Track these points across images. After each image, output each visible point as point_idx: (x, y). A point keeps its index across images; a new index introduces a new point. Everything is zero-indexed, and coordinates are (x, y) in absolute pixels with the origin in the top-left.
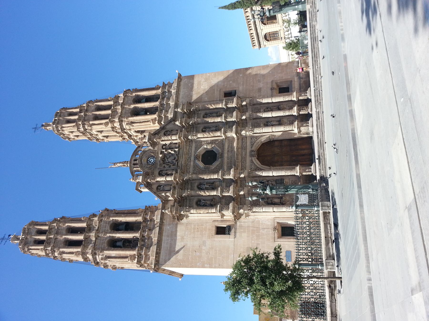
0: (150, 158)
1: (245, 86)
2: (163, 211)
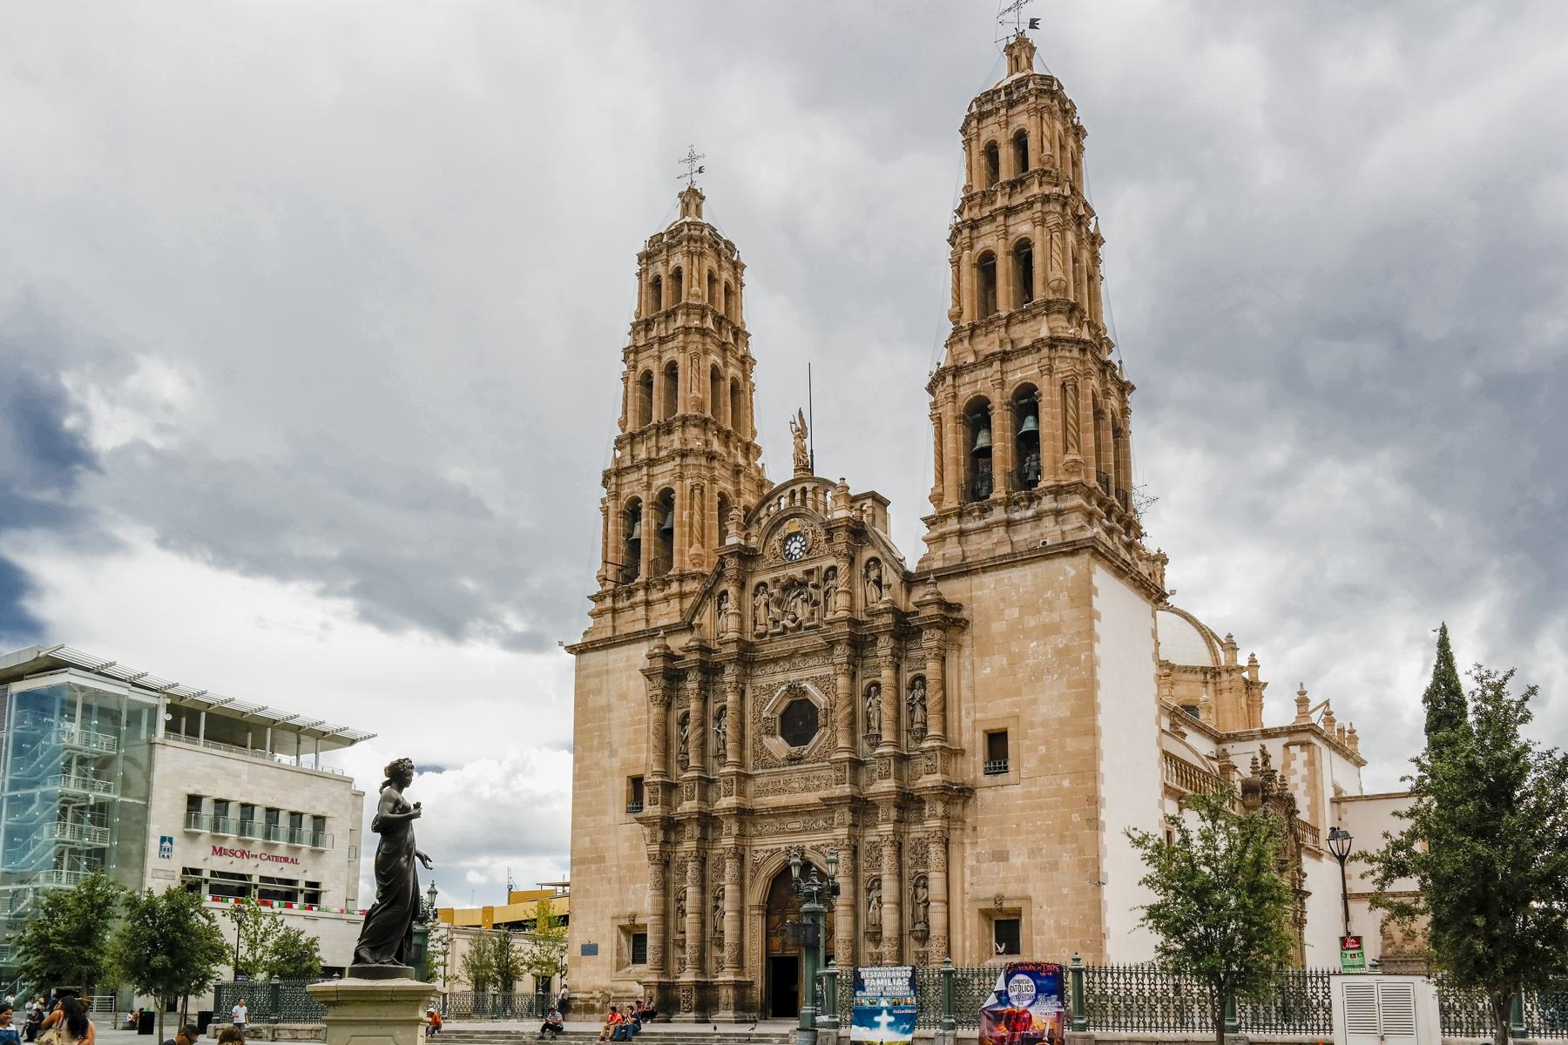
0: (802, 539)
1: (1021, 802)
2: (662, 632)
